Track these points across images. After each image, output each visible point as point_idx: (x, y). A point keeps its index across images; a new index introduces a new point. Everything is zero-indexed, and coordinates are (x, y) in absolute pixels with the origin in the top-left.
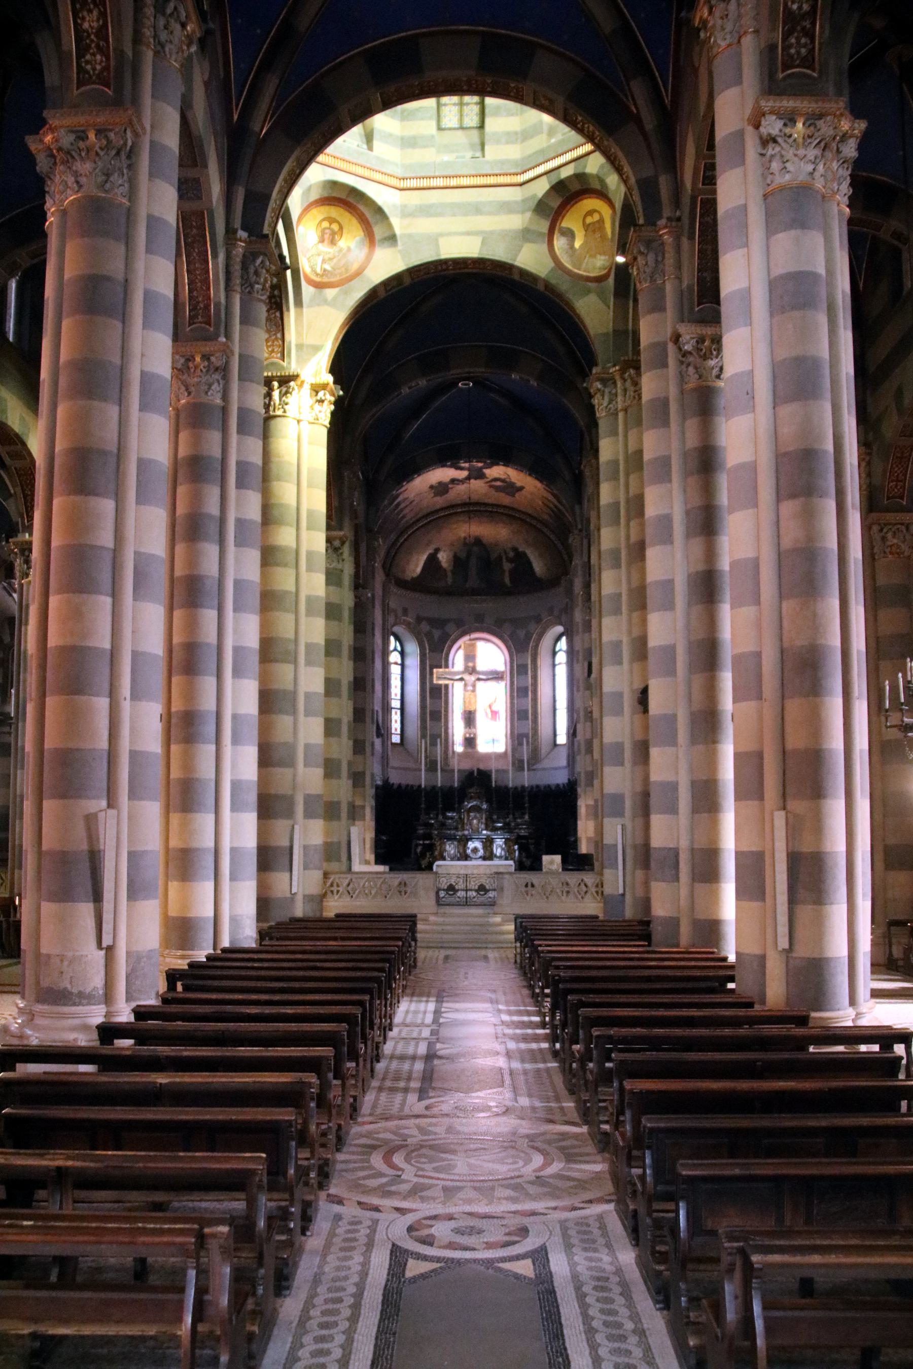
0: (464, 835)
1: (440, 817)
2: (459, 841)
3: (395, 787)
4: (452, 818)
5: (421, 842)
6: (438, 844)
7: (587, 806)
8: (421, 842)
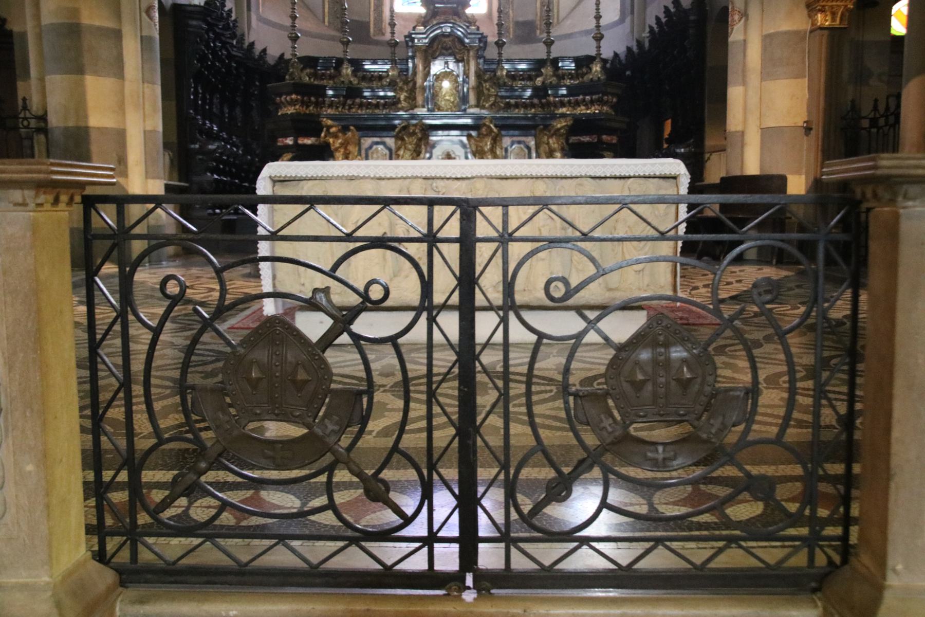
0: (413, 117)
1: (347, 70)
2: (402, 133)
3: (271, 62)
4: (380, 77)
5: (290, 141)
6: (335, 143)
7: (768, 40)
8: (290, 141)
